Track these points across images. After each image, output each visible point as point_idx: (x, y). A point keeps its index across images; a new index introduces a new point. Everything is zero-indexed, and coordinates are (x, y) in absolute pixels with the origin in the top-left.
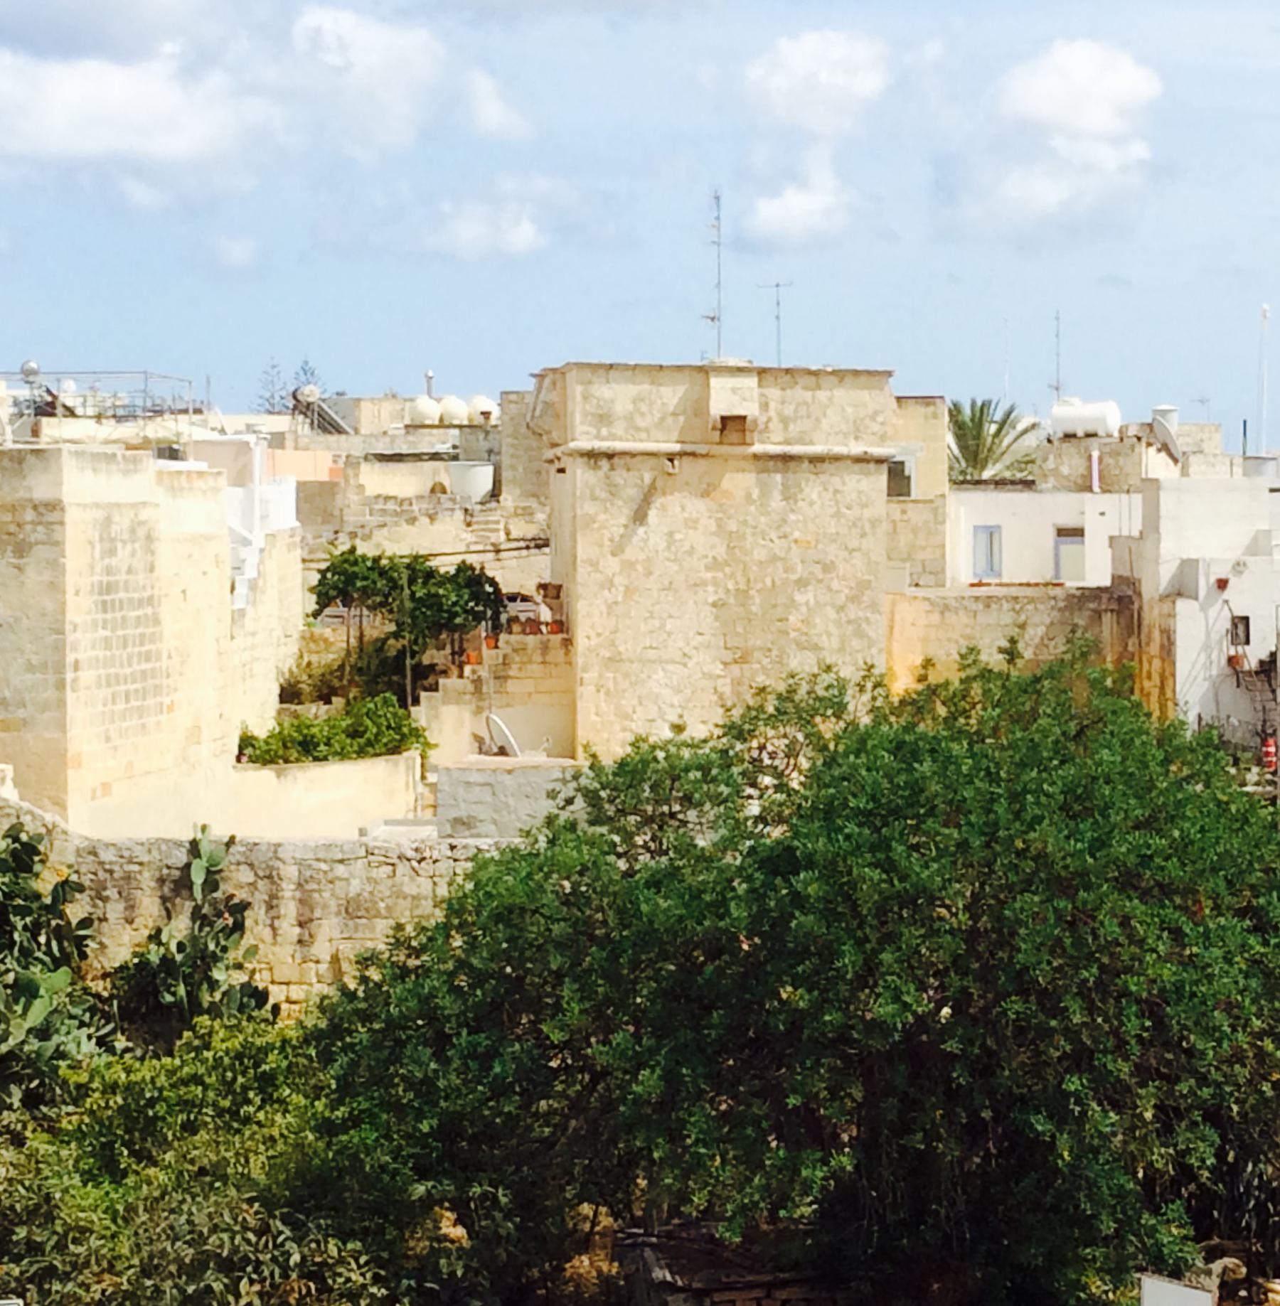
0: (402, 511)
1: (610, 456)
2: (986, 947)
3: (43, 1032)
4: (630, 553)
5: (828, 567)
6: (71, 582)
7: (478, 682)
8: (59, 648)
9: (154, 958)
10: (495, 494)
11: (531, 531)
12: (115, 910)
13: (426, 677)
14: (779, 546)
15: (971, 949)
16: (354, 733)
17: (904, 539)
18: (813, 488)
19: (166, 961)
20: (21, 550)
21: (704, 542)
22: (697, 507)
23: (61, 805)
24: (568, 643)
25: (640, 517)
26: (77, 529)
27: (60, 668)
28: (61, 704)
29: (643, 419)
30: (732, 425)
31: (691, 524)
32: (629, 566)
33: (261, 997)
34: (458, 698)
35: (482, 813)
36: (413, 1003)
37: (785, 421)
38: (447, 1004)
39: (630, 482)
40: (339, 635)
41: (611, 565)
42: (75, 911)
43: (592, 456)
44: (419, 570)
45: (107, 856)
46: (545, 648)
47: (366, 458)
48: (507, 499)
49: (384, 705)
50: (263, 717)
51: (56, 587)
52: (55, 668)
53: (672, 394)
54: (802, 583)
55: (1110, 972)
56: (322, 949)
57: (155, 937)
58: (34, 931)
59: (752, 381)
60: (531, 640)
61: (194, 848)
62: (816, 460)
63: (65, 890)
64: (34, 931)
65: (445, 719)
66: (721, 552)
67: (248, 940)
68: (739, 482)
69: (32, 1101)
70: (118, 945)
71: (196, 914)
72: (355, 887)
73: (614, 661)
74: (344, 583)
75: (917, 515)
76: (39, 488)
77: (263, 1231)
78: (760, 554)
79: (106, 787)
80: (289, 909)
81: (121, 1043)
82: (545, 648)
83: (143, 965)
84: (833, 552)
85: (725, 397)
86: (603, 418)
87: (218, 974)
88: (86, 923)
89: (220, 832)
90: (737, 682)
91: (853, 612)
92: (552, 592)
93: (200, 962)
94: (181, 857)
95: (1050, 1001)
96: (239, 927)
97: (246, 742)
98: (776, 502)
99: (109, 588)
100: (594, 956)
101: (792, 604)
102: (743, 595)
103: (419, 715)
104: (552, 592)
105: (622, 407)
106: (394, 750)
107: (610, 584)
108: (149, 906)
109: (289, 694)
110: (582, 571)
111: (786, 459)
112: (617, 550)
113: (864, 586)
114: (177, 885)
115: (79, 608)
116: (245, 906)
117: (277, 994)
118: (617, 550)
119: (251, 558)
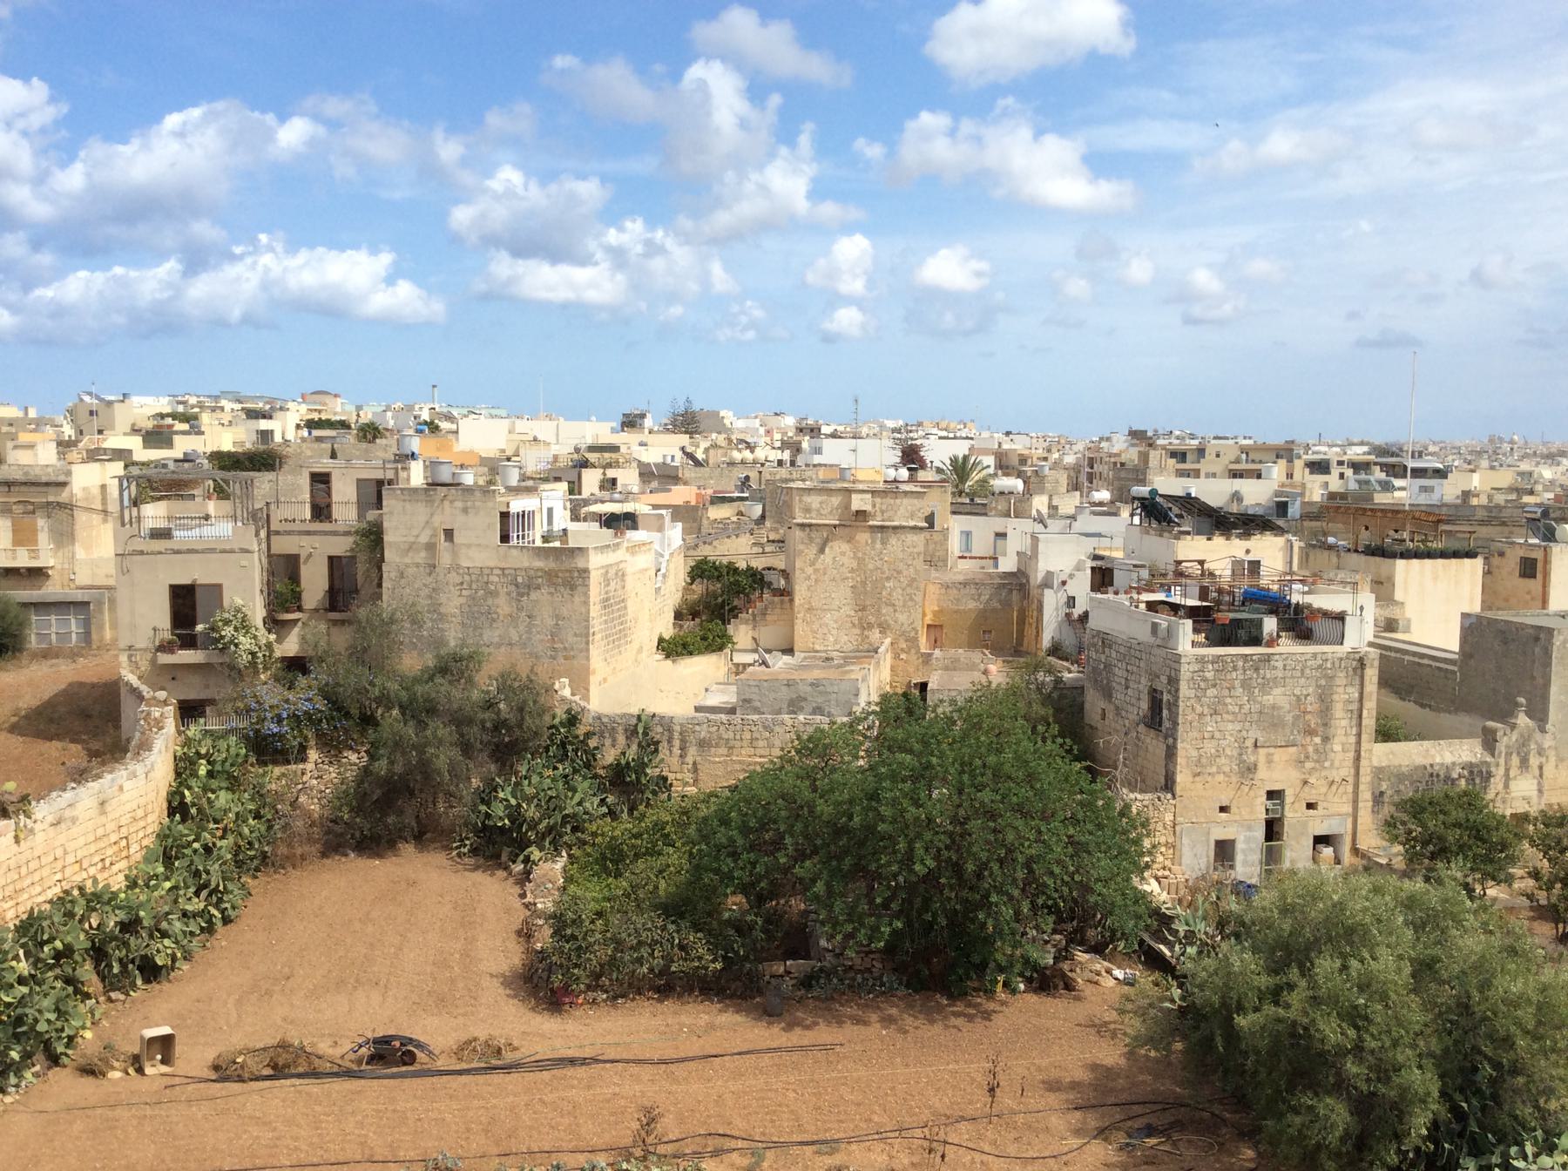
0: (725, 529)
1: (810, 525)
2: (958, 840)
3: (580, 804)
4: (818, 566)
5: (899, 572)
6: (592, 600)
7: (754, 615)
8: (587, 628)
9: (623, 762)
10: (763, 517)
11: (777, 537)
12: (608, 742)
13: (734, 612)
14: (879, 564)
15: (953, 842)
16: (704, 638)
17: (931, 547)
18: (893, 540)
19: (628, 763)
20: (573, 588)
21: (848, 561)
22: (845, 547)
23: (586, 698)
24: (792, 601)
25: (822, 551)
26: (595, 578)
27: (587, 635)
28: (588, 650)
29: (823, 510)
30: (861, 515)
31: (843, 554)
32: (816, 571)
33: (665, 779)
34: (746, 622)
35: (753, 697)
36: (724, 840)
37: (883, 512)
38: (740, 842)
39: (818, 537)
40: (699, 588)
41: (810, 570)
42: (592, 743)
43: (802, 526)
44: (732, 569)
45: (605, 720)
46: (782, 602)
47: (712, 503)
48: (768, 524)
49: (716, 625)
50: (667, 628)
51: (586, 603)
52: (586, 635)
53: (836, 500)
54: (888, 579)
55: (1010, 851)
56: (690, 759)
57: (624, 754)
58: (575, 751)
59: (869, 496)
60: (776, 599)
61: (639, 717)
62: (895, 528)
63: (588, 735)
64: (575, 751)
65: (741, 633)
66: (855, 565)
67: (661, 756)
68: (863, 537)
69: (575, 829)
70: (609, 756)
71: (639, 745)
72: (703, 734)
73: (810, 609)
74: (701, 571)
75: (936, 537)
76: (581, 564)
77: (664, 928)
78: (871, 566)
79: (605, 680)
80: (677, 743)
81: (610, 799)
82: (782, 602)
83: (619, 764)
84: (901, 566)
85: (858, 502)
86: (807, 510)
87: (648, 771)
88: (596, 748)
89: (651, 710)
90: (860, 619)
91: (909, 590)
92: (785, 574)
93: (641, 766)
94: (634, 721)
95: (984, 866)
96: (656, 751)
97: (661, 640)
98: (878, 546)
99: (607, 599)
100: (799, 827)
101: (884, 587)
102: (864, 583)
103: (731, 629)
104: (785, 574)
105: (815, 505)
106: (721, 649)
107: (809, 578)
108: (621, 739)
109: (678, 616)
110: (797, 572)
111: (882, 527)
112: (812, 564)
113: (914, 580)
114: (631, 732)
115: (595, 610)
116: (658, 742)
117: (671, 776)
118: (812, 564)
119: (664, 561)
